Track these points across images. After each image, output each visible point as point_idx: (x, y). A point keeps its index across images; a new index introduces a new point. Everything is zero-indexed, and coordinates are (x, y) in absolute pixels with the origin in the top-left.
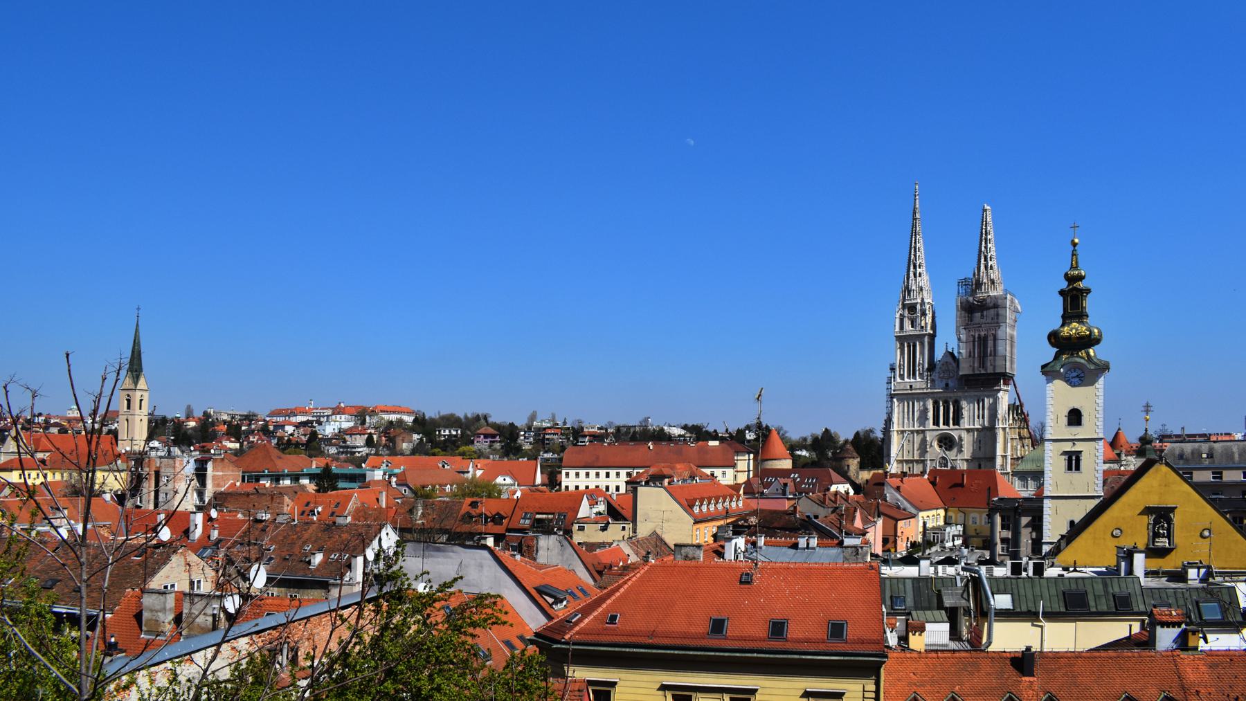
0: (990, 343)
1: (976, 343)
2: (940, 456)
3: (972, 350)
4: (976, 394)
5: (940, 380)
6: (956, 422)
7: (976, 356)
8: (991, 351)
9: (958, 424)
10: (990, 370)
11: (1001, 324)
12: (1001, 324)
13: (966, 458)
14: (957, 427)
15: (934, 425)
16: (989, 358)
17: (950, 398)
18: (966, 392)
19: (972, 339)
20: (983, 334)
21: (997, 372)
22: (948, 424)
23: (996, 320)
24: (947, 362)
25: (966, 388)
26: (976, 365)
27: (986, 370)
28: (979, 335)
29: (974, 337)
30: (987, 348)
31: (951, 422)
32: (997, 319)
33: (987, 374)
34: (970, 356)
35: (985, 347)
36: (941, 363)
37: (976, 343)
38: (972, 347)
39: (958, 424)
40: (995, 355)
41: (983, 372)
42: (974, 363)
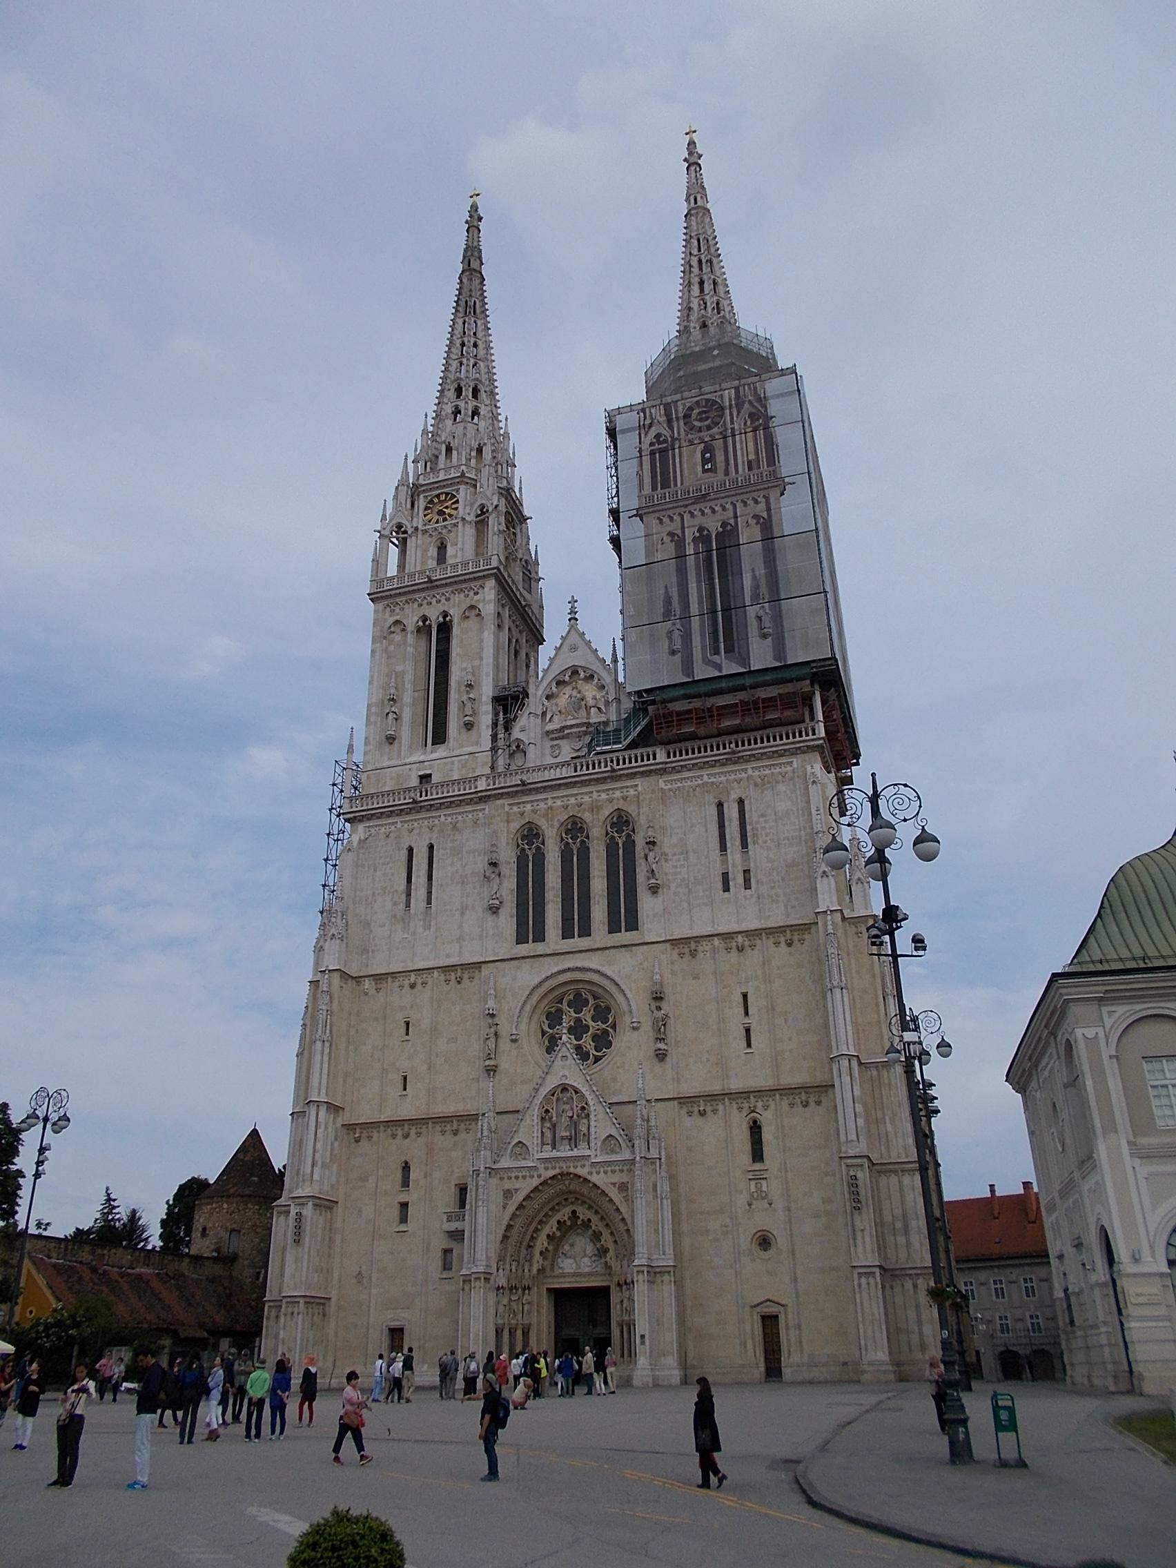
1: (691, 561)
2: (552, 1082)
4: (706, 776)
5: (548, 744)
7: (694, 609)
8: (756, 588)
10: (761, 656)
13: (688, 1089)
14: (625, 937)
15: (521, 939)
16: (752, 612)
17: (595, 808)
18: (663, 772)
19: (671, 549)
20: (713, 526)
21: (789, 662)
22: (586, 931)
24: (575, 672)
25: (661, 756)
27: (745, 660)
28: (701, 529)
29: (680, 543)
31: (599, 912)
32: (772, 459)
33: (750, 672)
34: (667, 614)
36: (550, 677)
37: (691, 561)
38: (674, 579)
39: (633, 925)
40: (776, 600)
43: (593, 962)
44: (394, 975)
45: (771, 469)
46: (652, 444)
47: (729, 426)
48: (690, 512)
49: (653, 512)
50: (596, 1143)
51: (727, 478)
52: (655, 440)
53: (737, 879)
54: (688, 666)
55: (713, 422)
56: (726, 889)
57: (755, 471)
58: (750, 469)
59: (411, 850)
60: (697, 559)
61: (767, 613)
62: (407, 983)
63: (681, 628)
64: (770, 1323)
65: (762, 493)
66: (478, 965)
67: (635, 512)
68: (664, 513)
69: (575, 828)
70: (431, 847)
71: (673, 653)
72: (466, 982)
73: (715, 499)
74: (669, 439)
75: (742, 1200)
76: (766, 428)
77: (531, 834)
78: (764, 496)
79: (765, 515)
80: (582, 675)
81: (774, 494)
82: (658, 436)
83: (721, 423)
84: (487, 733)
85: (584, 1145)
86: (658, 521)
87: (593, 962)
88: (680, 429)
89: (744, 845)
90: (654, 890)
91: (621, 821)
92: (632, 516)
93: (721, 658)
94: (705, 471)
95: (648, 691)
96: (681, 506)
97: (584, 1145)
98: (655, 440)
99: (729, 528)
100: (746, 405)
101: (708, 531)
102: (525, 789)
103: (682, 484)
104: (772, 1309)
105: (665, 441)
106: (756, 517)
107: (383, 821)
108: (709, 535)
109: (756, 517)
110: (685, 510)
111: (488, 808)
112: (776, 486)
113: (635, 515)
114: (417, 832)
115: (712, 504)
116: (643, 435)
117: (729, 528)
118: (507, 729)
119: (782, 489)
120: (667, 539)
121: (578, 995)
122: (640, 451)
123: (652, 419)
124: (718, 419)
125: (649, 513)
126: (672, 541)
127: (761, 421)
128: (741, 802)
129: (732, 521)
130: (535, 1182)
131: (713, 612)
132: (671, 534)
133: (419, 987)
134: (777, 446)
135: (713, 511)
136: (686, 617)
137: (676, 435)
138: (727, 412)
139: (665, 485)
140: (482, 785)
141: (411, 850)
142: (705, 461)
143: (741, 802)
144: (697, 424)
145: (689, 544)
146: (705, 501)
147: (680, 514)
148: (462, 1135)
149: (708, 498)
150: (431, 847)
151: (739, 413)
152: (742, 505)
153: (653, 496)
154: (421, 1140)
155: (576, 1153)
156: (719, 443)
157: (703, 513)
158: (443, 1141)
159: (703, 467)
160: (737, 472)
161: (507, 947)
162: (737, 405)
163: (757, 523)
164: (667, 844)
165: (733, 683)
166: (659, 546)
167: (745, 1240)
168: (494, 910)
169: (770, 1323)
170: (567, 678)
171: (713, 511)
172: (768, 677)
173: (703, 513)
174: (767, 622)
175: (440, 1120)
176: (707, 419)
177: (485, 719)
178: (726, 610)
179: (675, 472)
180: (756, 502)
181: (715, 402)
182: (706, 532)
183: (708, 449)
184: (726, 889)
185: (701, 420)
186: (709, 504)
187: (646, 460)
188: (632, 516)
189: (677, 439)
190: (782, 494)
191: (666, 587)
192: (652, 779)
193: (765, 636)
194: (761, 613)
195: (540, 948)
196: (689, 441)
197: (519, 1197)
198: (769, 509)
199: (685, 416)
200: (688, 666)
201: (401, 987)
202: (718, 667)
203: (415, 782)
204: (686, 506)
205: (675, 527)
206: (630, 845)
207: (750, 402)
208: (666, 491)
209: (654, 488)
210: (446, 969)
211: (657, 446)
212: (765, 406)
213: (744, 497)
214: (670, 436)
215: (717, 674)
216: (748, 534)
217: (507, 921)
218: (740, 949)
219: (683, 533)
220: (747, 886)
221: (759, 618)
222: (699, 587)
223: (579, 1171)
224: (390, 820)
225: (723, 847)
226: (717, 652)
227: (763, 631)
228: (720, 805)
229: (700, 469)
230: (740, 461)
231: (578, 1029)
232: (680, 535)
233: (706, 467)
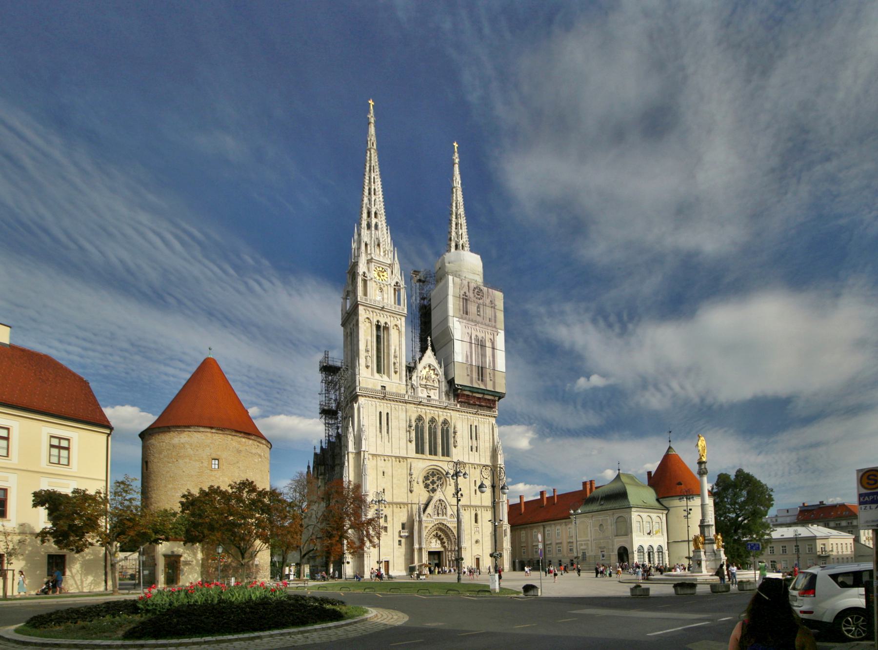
0: (489, 351)
1: (473, 345)
3: (469, 354)
6: (446, 452)
7: (474, 364)
8: (490, 363)
9: (448, 455)
10: (490, 388)
11: (499, 331)
12: (499, 331)
15: (417, 452)
16: (488, 371)
19: (468, 339)
21: (497, 390)
23: (494, 324)
26: (475, 375)
27: (485, 385)
28: (476, 336)
32: (495, 322)
33: (487, 390)
34: (467, 361)
35: (484, 355)
37: (473, 345)
38: (469, 350)
40: (494, 370)
41: (482, 387)
42: (472, 371)
43: (440, 464)
44: (379, 455)
50: (448, 516)
53: (474, 449)
56: (472, 450)
59: (380, 413)
62: (383, 459)
64: (478, 559)
66: (406, 458)
69: (433, 420)
70: (388, 414)
72: (402, 462)
75: (473, 532)
76: (494, 308)
77: (420, 419)
80: (432, 368)
81: (495, 334)
82: (465, 293)
84: (404, 378)
85: (445, 516)
87: (440, 464)
89: (476, 439)
90: (455, 447)
91: (445, 422)
93: (480, 382)
94: (478, 315)
95: (461, 385)
97: (445, 516)
100: (489, 297)
102: (420, 403)
104: (478, 557)
105: (467, 296)
106: (490, 339)
107: (371, 399)
109: (490, 339)
111: (409, 406)
114: (384, 407)
118: (411, 378)
121: (433, 472)
127: (493, 305)
128: (476, 426)
130: (433, 525)
133: (387, 461)
136: (471, 365)
139: (467, 313)
140: (406, 398)
141: (380, 413)
142: (478, 311)
143: (476, 426)
144: (477, 296)
148: (403, 509)
150: (388, 414)
154: (391, 509)
155: (443, 518)
156: (481, 307)
158: (397, 510)
164: (458, 434)
165: (484, 392)
167: (474, 542)
168: (410, 441)
169: (478, 559)
170: (432, 368)
172: (490, 393)
174: (491, 375)
175: (397, 504)
176: (479, 295)
177: (404, 373)
178: (482, 368)
181: (482, 290)
183: (478, 307)
184: (472, 450)
187: (461, 300)
192: (455, 412)
193: (491, 380)
195: (424, 456)
197: (429, 528)
199: (474, 290)
201: (381, 460)
202: (479, 385)
203: (380, 388)
206: (447, 431)
209: (464, 313)
210: (396, 457)
211: (464, 297)
215: (478, 387)
216: (488, 344)
217: (413, 446)
218: (475, 468)
220: (477, 451)
223: (444, 523)
224: (373, 400)
225: (471, 438)
226: (479, 380)
228: (471, 426)
231: (433, 482)
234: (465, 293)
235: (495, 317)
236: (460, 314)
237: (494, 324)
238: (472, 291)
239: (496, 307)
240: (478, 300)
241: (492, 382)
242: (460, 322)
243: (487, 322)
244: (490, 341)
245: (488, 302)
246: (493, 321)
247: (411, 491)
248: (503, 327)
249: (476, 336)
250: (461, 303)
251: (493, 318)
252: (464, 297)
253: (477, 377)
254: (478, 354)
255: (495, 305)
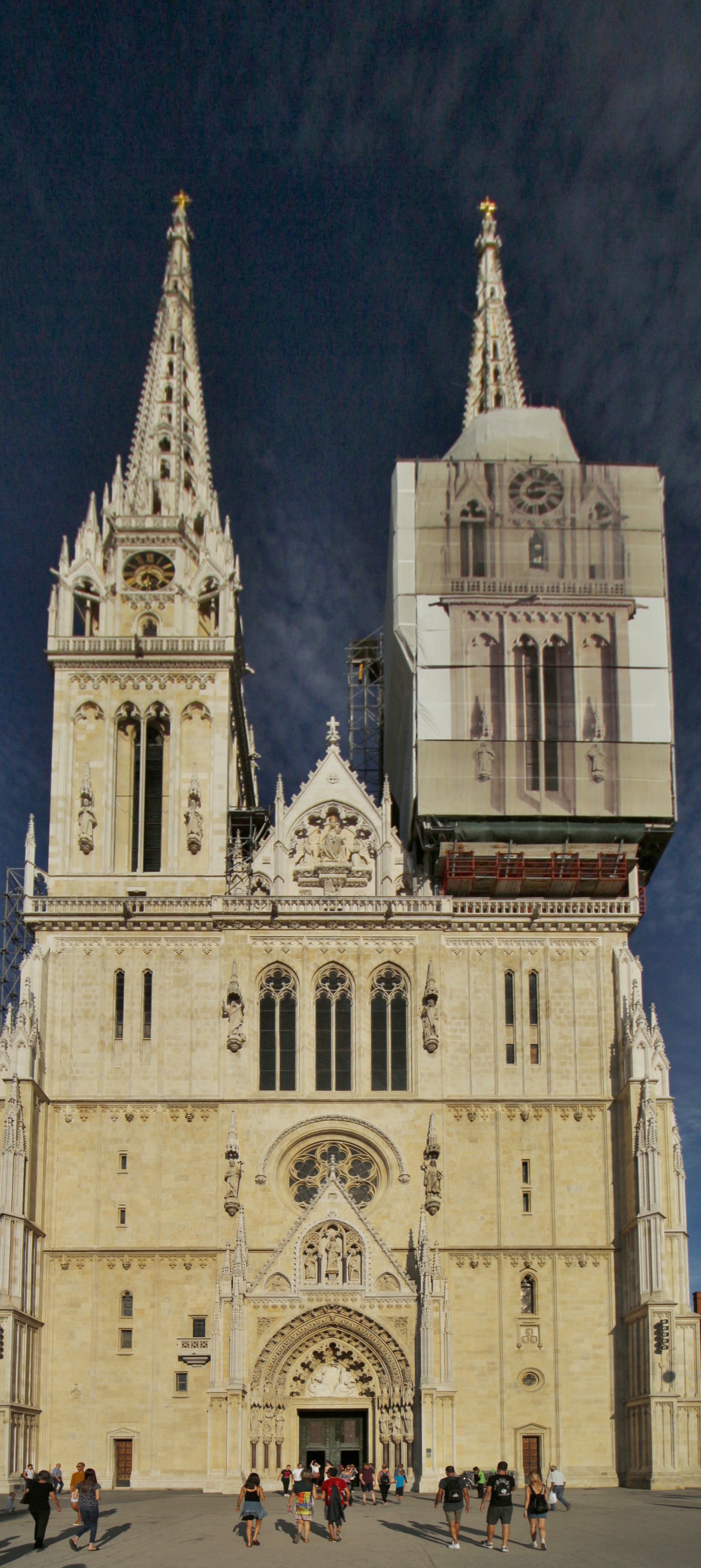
3: (487, 707)
7: (511, 732)
12: (639, 601)
16: (582, 750)
20: (542, 635)
21: (625, 812)
23: (611, 582)
27: (569, 802)
28: (525, 638)
29: (497, 650)
30: (571, 700)
32: (621, 572)
34: (477, 730)
37: (510, 675)
38: (487, 692)
41: (552, 808)
42: (499, 761)
45: (619, 582)
46: (464, 513)
47: (569, 514)
48: (512, 614)
49: (462, 604)
51: (561, 581)
52: (468, 509)
54: (499, 795)
55: (549, 503)
57: (598, 580)
58: (592, 575)
60: (518, 674)
61: (601, 755)
63: (492, 752)
65: (606, 610)
67: (436, 599)
68: (477, 608)
71: (482, 778)
73: (545, 605)
74: (488, 513)
76: (617, 527)
78: (608, 615)
79: (608, 638)
81: (621, 615)
82: (473, 504)
83: (559, 507)
86: (469, 617)
88: (503, 502)
92: (434, 604)
93: (541, 795)
94: (533, 566)
96: (499, 604)
98: (468, 509)
99: (561, 644)
101: (534, 641)
103: (502, 575)
105: (482, 514)
106: (597, 638)
108: (534, 649)
109: (597, 638)
110: (504, 609)
112: (624, 606)
113: (440, 604)
115: (542, 610)
116: (452, 497)
117: (561, 644)
119: (631, 610)
120: (481, 642)
122: (448, 519)
123: (467, 480)
124: (554, 500)
125: (457, 604)
126: (487, 644)
127: (610, 518)
129: (565, 637)
131: (534, 741)
132: (486, 637)
134: (629, 555)
135: (542, 619)
137: (497, 510)
138: (567, 495)
139: (480, 571)
142: (533, 553)
145: (509, 653)
146: (531, 605)
147: (498, 614)
149: (536, 602)
151: (583, 499)
152: (579, 619)
153: (463, 583)
157: (529, 619)
159: (531, 559)
160: (575, 576)
161: (251, 1085)
162: (582, 489)
163: (598, 646)
166: (470, 648)
171: (542, 619)
173: (529, 619)
179: (493, 558)
180: (598, 620)
181: (552, 477)
182: (530, 643)
183: (538, 539)
185: (532, 496)
186: (536, 609)
187: (455, 534)
188: (434, 604)
189: (498, 515)
190: (631, 617)
191: (477, 699)
193: (596, 779)
194: (593, 753)
196: (514, 522)
198: (613, 635)
199: (514, 486)
200: (499, 795)
202: (537, 805)
204: (507, 606)
205: (492, 629)
207: (600, 490)
208: (481, 580)
209: (465, 573)
211: (470, 518)
212: (617, 499)
213: (583, 610)
214: (490, 509)
219: (502, 635)
221: (591, 758)
222: (519, 707)
226: (535, 786)
227: (594, 773)
229: (527, 561)
230: (579, 562)
232: (497, 639)
233: (535, 561)
234: (473, 504)
235: (621, 555)
236: (445, 580)
237: (611, 582)
238: (506, 492)
239: (627, 524)
240: (535, 517)
241: (601, 786)
242: (446, 607)
243: (582, 579)
244: (592, 643)
245: (584, 511)
246: (610, 572)
247: (232, 1210)
248: (661, 582)
249: (525, 638)
250: (455, 544)
251: (610, 562)
252: (470, 518)
253: (526, 776)
254: (535, 697)
255: (620, 517)
